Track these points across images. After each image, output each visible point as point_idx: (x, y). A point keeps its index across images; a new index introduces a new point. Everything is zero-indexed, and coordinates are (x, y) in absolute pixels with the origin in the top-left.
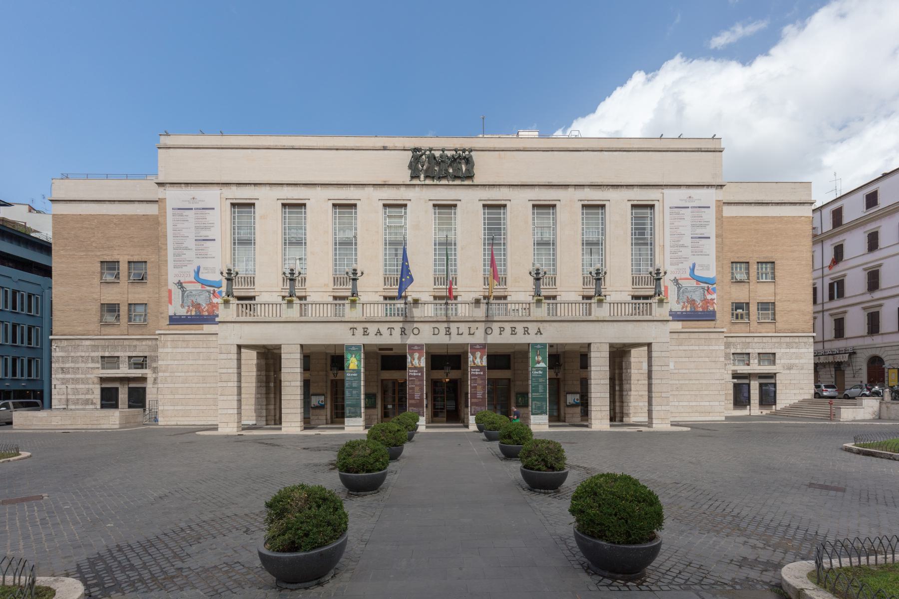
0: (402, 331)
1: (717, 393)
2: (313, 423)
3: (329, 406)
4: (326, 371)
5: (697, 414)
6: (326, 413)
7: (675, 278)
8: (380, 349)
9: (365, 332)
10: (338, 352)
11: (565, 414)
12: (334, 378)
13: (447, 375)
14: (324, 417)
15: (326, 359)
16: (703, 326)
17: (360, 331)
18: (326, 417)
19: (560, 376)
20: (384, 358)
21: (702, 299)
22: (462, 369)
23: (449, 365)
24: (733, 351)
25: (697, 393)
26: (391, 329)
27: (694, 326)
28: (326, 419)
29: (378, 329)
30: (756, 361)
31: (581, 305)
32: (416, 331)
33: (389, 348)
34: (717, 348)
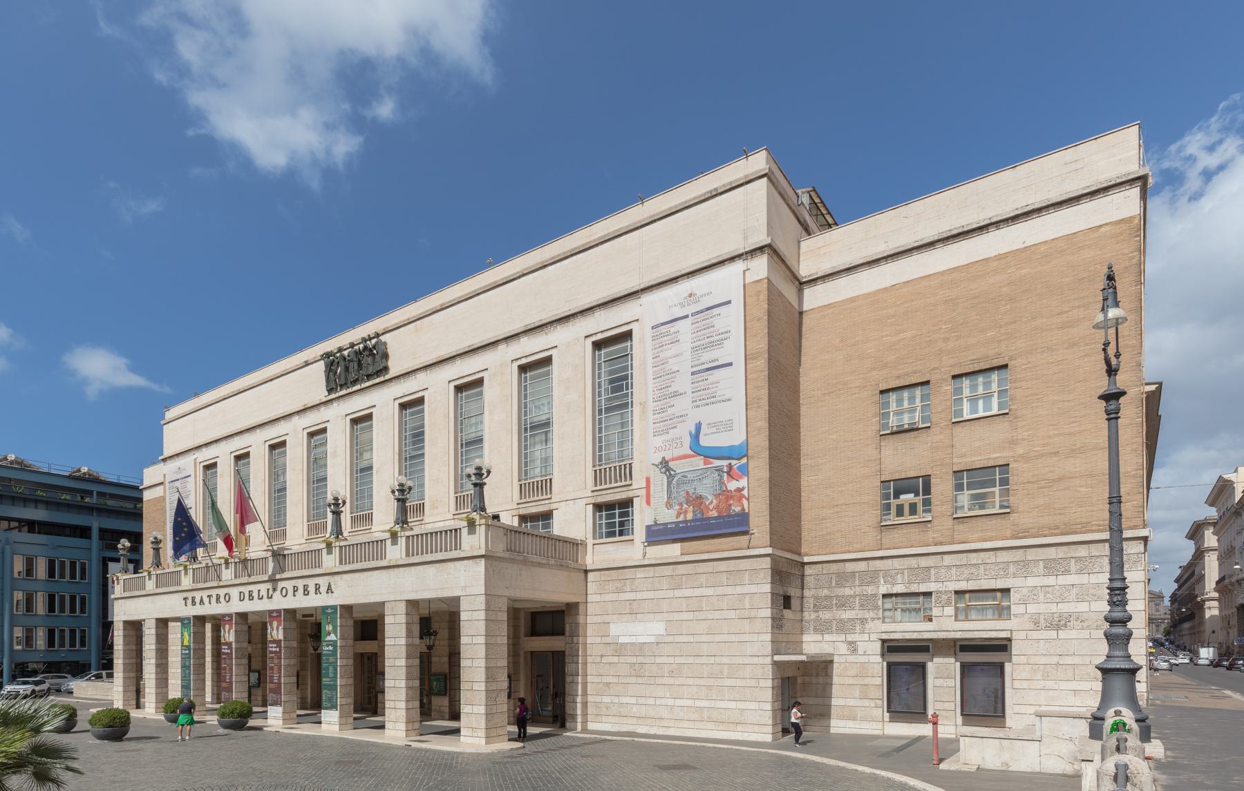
1: (753, 683)
5: (711, 726)
7: (664, 458)
16: (724, 547)
21: (718, 492)
24: (883, 589)
25: (711, 682)
27: (705, 548)
30: (950, 611)
34: (753, 589)
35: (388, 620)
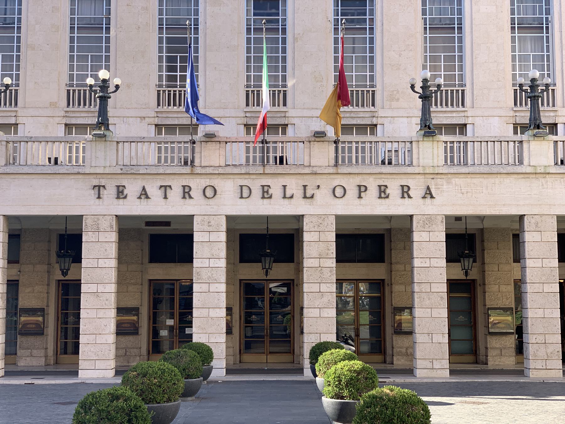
0: (184, 192)
2: (22, 364)
3: (51, 330)
4: (49, 264)
6: (47, 344)
8: (148, 224)
9: (120, 193)
10: (72, 229)
11: (487, 348)
12: (62, 278)
13: (267, 272)
14: (42, 353)
15: (49, 241)
17: (110, 193)
18: (46, 352)
19: (474, 275)
20: (155, 240)
22: (295, 261)
23: (270, 255)
26: (165, 188)
28: (46, 356)
29: (144, 189)
31: (511, 144)
32: (209, 193)
33: (164, 221)
35: (307, 237)
